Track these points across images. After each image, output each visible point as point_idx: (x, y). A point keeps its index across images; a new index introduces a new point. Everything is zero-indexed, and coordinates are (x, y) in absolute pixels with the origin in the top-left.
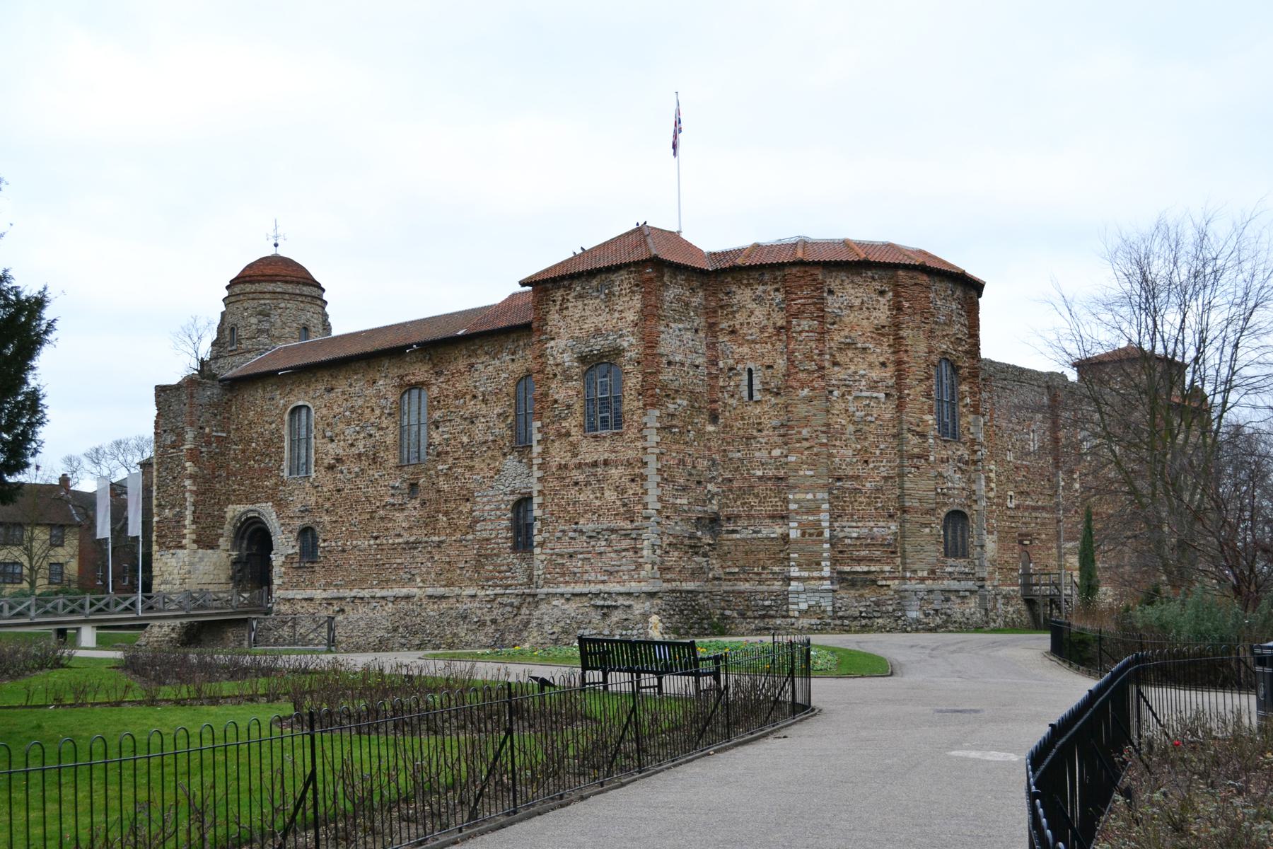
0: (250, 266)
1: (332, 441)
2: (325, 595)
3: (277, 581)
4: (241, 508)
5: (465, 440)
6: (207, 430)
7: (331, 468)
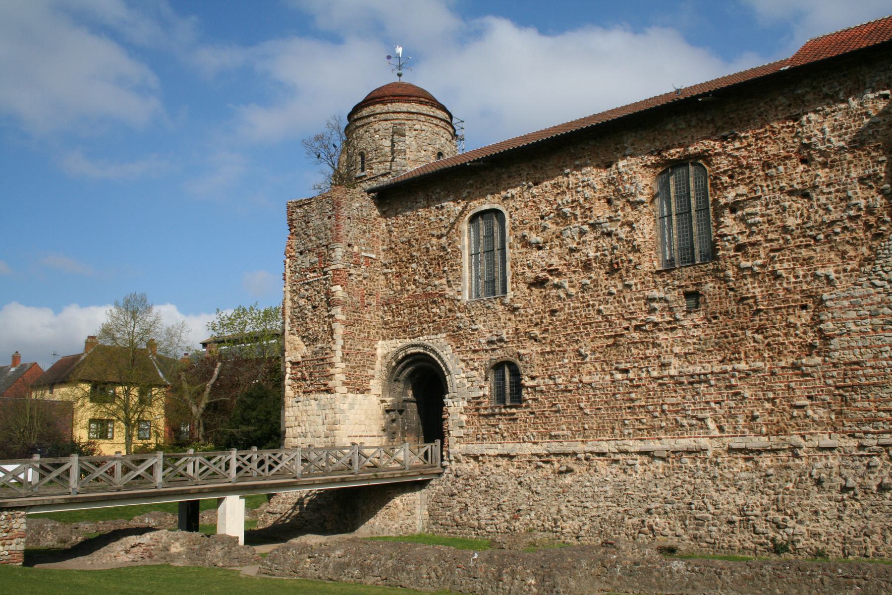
0: (378, 90)
1: (540, 248)
2: (540, 449)
3: (455, 432)
4: (399, 343)
5: (791, 222)
6: (356, 249)
7: (539, 283)
